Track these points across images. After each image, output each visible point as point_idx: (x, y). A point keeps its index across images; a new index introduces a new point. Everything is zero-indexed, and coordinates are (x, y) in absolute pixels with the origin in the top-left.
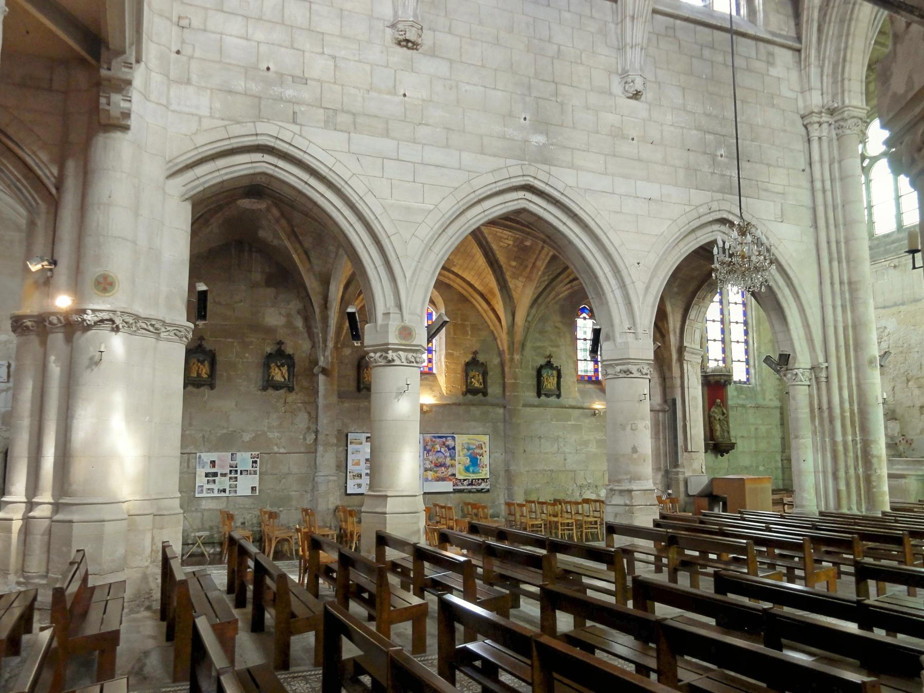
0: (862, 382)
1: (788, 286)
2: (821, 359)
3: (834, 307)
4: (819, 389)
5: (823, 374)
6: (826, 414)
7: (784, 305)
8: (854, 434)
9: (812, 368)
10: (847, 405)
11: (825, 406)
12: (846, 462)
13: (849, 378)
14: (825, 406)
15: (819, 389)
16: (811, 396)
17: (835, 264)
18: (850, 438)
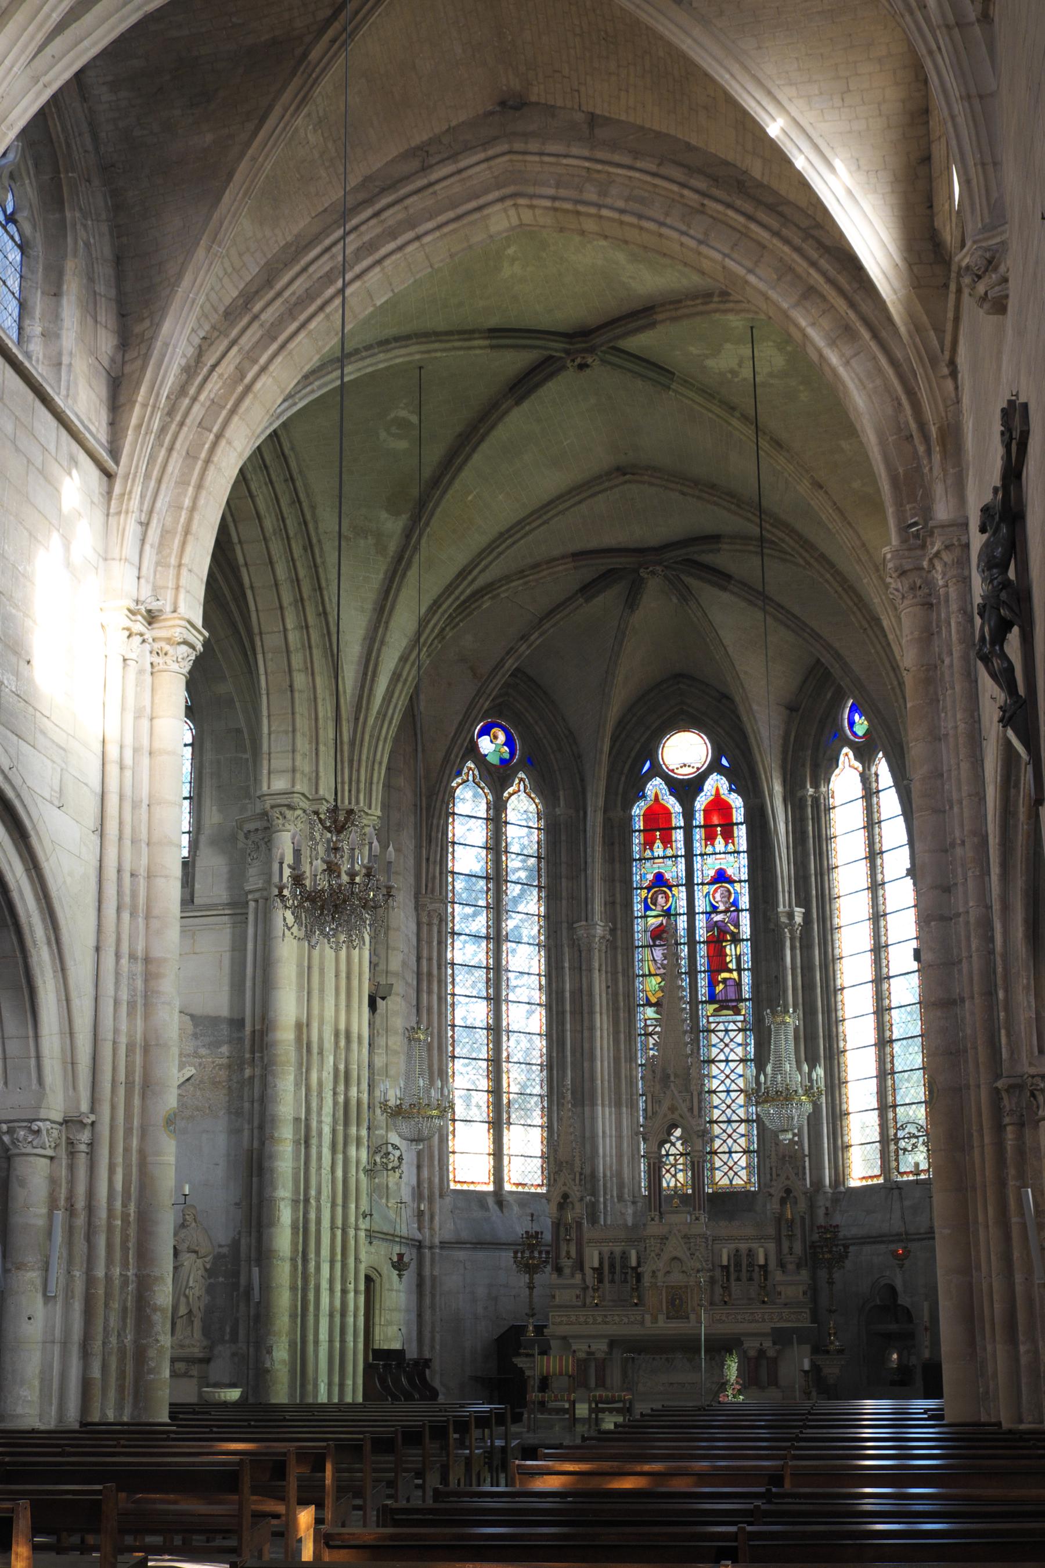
0: (150, 1159)
1: (49, 943)
2: (85, 1107)
3: (116, 1002)
4: (71, 1168)
5: (85, 1136)
6: (80, 1221)
7: (39, 982)
8: (125, 1265)
9: (66, 1122)
10: (118, 1204)
11: (80, 1203)
12: (106, 1319)
13: (127, 1150)
14: (80, 1203)
15: (71, 1168)
16: (53, 1181)
17: (126, 916)
18: (117, 1271)
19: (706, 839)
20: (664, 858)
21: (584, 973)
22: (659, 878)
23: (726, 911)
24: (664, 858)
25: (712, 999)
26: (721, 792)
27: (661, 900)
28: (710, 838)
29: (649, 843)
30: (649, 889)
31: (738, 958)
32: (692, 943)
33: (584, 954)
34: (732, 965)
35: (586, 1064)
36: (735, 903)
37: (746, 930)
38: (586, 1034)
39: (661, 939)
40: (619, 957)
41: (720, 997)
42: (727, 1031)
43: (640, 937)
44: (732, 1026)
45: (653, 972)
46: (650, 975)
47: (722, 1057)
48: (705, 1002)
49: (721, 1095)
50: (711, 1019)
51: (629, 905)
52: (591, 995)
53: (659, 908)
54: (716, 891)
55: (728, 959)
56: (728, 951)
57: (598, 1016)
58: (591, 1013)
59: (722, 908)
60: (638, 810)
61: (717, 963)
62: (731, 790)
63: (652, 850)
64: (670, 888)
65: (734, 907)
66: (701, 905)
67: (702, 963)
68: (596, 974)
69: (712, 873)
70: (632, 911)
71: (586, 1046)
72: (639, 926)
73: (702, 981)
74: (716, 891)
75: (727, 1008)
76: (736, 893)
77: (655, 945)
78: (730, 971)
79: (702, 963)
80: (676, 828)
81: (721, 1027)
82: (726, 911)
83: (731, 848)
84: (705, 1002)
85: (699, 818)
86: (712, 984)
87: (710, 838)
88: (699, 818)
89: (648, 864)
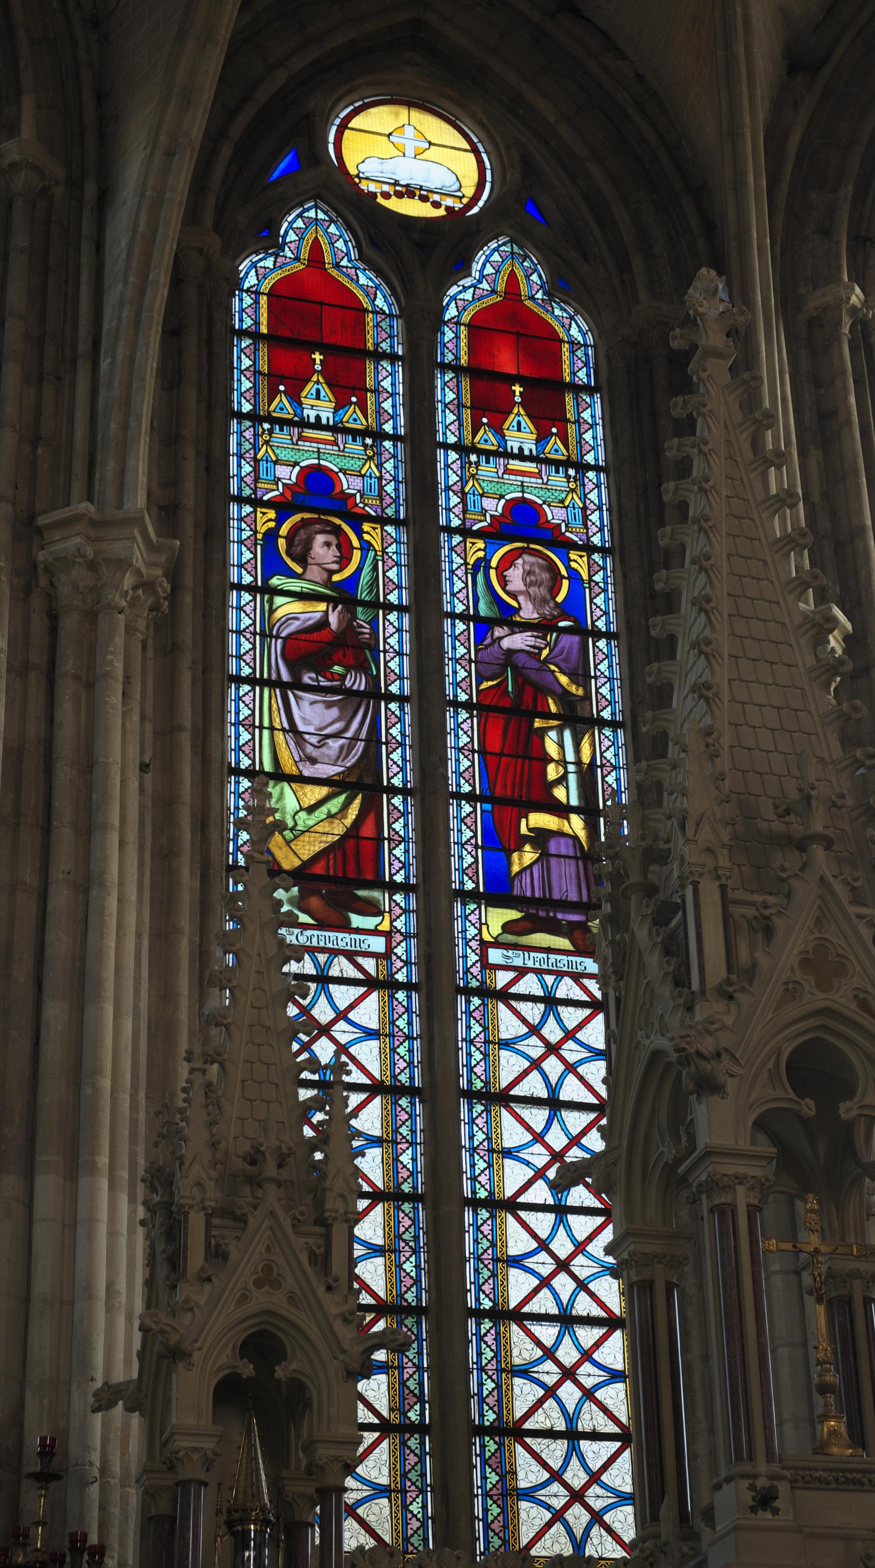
19: (478, 410)
20: (334, 429)
21: (67, 689)
22: (317, 483)
23: (543, 627)
24: (334, 429)
25: (498, 890)
26: (524, 290)
27: (322, 550)
28: (489, 407)
29: (287, 378)
30: (283, 508)
31: (588, 776)
32: (428, 699)
33: (69, 624)
34: (568, 794)
35: (55, 1012)
36: (574, 607)
37: (607, 693)
38: (61, 899)
39: (322, 669)
40: (186, 679)
41: (524, 888)
42: (551, 1002)
43: (243, 653)
44: (567, 989)
45: (289, 767)
46: (279, 776)
47: (533, 1086)
48: (473, 896)
49: (534, 1219)
50: (495, 956)
51: (215, 535)
52: (89, 764)
53: (314, 573)
54: (508, 562)
55: (552, 772)
56: (552, 748)
57: (114, 838)
58: (88, 828)
59: (528, 612)
60: (258, 272)
61: (515, 782)
62: (555, 290)
63: (295, 397)
64: (357, 521)
65: (567, 619)
66: (457, 591)
67: (462, 768)
68: (115, 699)
69: (494, 507)
70: (225, 564)
71: (60, 941)
72: (242, 612)
73: (465, 826)
74: (508, 562)
75: (554, 929)
76: (574, 576)
77: (297, 685)
78: (562, 810)
79: (462, 768)
80: (378, 356)
81: (530, 985)
82: (543, 627)
83: (555, 448)
84: (473, 896)
85: (454, 344)
86: (498, 841)
87: (489, 407)
88: (454, 344)
89: (281, 437)
